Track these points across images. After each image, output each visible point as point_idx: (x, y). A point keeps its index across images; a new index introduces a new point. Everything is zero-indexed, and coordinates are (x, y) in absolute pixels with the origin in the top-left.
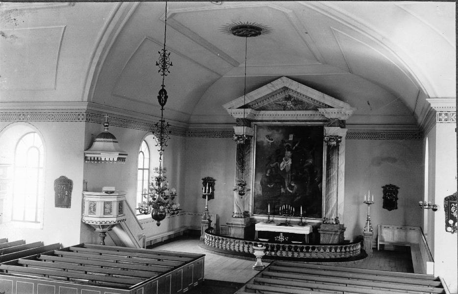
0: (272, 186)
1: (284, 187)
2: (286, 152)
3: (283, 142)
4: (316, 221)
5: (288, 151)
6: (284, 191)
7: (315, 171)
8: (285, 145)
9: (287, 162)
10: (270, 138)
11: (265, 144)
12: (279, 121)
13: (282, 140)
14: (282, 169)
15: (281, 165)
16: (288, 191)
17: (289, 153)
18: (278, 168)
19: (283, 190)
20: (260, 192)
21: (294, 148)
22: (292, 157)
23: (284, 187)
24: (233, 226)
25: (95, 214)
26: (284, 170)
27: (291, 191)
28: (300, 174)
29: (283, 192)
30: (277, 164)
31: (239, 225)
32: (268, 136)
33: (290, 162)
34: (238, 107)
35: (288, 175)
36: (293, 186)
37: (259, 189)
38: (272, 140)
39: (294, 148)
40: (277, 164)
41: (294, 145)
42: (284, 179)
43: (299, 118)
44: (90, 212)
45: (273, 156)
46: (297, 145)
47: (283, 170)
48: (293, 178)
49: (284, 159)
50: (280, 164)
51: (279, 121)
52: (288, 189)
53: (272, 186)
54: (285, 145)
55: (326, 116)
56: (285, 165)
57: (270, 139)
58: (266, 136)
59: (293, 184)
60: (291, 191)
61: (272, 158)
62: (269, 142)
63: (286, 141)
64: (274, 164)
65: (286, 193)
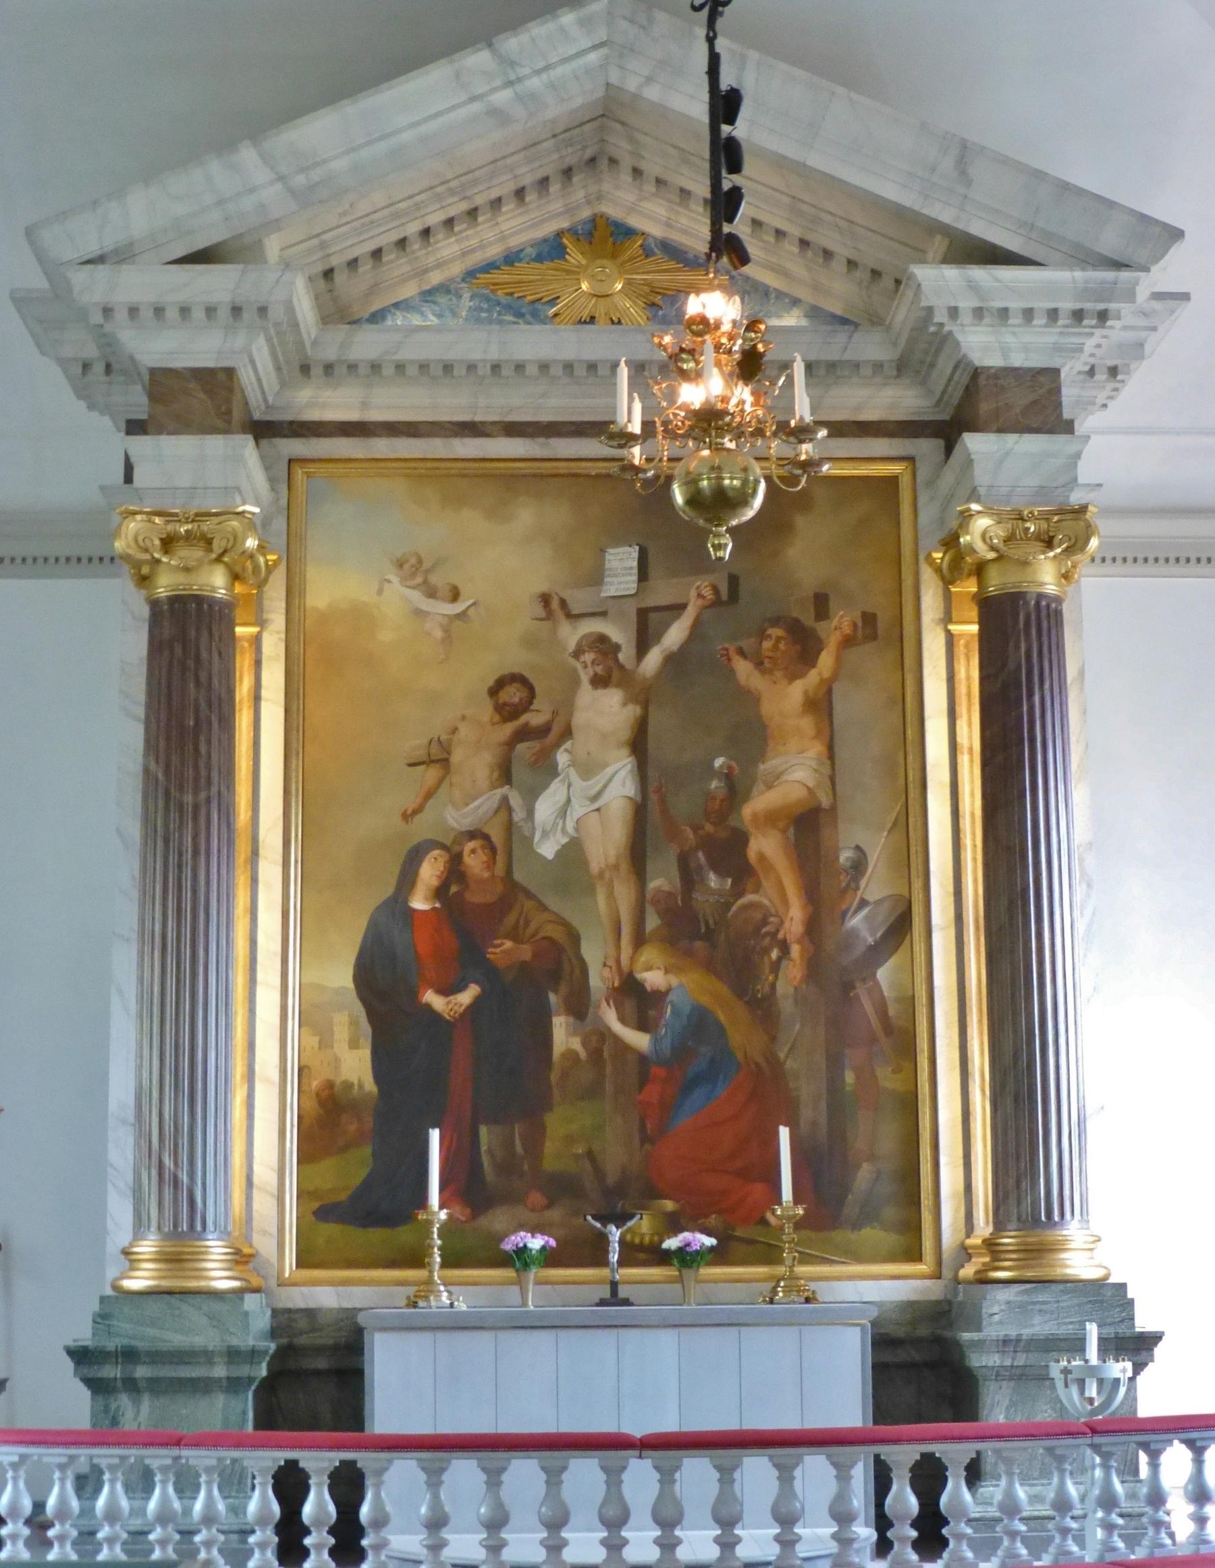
0: (466, 997)
1: (579, 1007)
2: (586, 695)
3: (551, 606)
4: (877, 1286)
5: (600, 682)
6: (576, 1044)
7: (845, 856)
8: (572, 635)
10: (435, 579)
11: (385, 636)
12: (513, 429)
13: (545, 599)
14: (548, 849)
15: (545, 808)
16: (617, 1039)
17: (604, 713)
18: (505, 839)
19: (564, 1036)
20: (356, 1066)
21: (654, 659)
22: (638, 744)
23: (579, 1007)
24: (141, 1372)
26: (573, 852)
27: (640, 1040)
28: (713, 880)
29: (571, 1055)
30: (505, 801)
31: (207, 1356)
32: (414, 568)
33: (620, 782)
34: (180, 253)
35: (611, 896)
36: (658, 997)
37: (341, 1033)
38: (455, 595)
39: (654, 659)
40: (505, 801)
41: (642, 647)
42: (575, 939)
45: (465, 731)
46: (675, 635)
47: (563, 853)
48: (652, 922)
49: (562, 758)
50: (530, 813)
51: (513, 429)
52: (611, 1017)
53: (466, 997)
54: (572, 635)
55: (983, 346)
56: (578, 809)
57: (431, 593)
58: (400, 564)
59: (654, 978)
60: (640, 1040)
61: (457, 757)
62: (419, 613)
63: (579, 600)
64: (487, 802)
65: (596, 1055)
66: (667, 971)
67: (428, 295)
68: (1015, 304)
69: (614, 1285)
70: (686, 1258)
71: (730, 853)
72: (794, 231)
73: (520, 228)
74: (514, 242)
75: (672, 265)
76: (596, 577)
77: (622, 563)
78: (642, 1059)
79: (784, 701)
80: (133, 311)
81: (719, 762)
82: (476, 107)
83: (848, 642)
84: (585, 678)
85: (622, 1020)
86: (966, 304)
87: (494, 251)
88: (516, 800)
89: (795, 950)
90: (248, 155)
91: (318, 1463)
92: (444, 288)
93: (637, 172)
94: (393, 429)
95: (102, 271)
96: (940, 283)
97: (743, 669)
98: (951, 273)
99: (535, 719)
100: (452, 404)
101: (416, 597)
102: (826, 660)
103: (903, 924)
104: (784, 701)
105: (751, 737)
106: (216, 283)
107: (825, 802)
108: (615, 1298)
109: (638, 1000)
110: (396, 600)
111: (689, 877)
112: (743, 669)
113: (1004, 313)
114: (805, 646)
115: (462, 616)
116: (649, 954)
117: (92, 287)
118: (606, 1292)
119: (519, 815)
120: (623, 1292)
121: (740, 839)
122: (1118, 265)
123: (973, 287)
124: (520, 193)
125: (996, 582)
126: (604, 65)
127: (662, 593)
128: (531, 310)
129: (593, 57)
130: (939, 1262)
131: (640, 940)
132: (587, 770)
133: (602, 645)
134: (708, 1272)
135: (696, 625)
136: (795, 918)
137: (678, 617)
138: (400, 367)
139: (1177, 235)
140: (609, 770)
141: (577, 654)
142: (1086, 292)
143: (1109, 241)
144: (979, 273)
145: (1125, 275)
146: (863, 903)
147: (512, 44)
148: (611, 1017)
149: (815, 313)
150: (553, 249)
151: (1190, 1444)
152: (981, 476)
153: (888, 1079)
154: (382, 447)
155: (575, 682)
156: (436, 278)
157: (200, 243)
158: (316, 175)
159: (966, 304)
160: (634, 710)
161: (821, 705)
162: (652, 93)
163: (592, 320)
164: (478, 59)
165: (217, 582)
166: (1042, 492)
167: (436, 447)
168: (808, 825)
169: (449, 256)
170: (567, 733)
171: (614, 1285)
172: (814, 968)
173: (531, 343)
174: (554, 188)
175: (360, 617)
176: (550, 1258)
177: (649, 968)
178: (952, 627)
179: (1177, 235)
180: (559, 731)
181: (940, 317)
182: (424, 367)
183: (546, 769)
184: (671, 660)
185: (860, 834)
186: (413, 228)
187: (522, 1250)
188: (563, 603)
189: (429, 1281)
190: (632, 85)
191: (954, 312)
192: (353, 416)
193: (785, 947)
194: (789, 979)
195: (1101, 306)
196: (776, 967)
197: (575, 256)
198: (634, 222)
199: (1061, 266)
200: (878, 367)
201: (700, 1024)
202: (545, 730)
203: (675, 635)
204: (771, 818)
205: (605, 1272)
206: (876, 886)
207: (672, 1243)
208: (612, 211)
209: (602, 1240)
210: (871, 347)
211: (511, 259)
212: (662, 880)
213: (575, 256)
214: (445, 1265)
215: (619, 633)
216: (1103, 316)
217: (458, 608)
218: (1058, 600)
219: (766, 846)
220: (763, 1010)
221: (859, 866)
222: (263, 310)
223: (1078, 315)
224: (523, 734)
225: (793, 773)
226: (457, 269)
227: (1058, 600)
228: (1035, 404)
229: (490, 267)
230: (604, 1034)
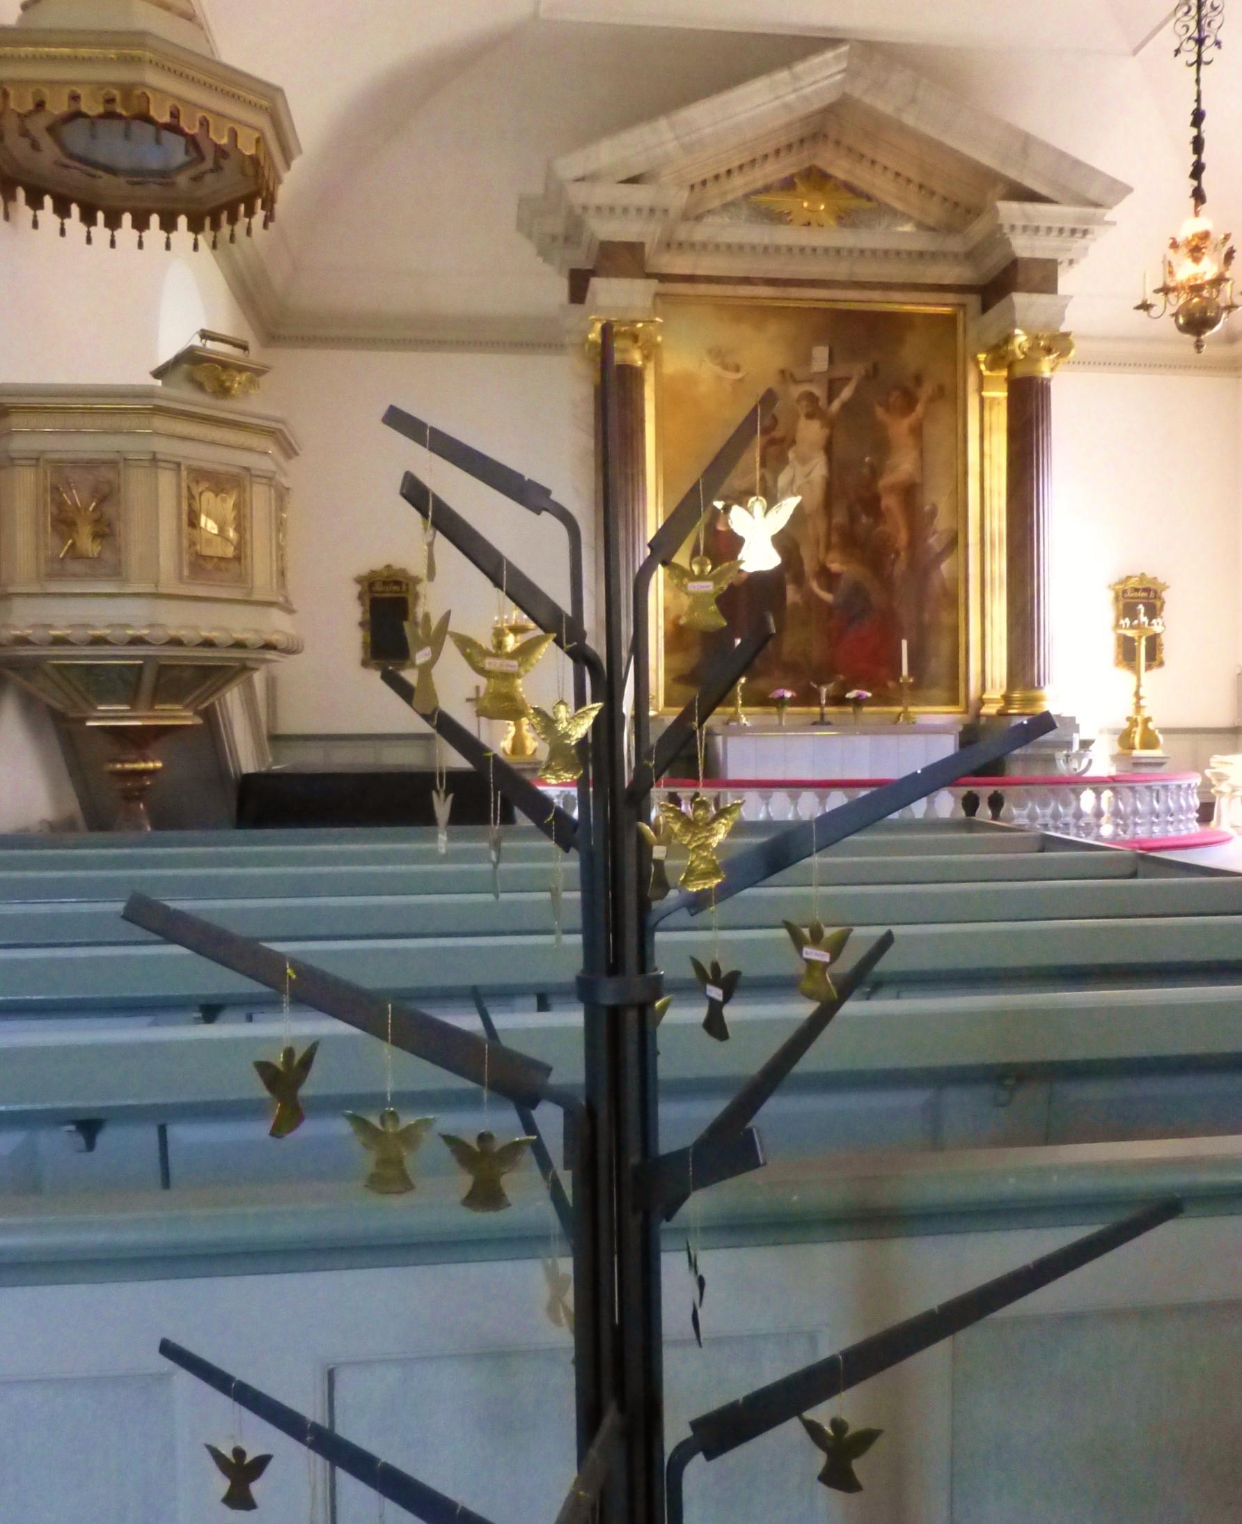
5: (810, 416)
7: (927, 508)
8: (796, 391)
9: (806, 469)
13: (782, 372)
17: (811, 432)
21: (836, 405)
22: (829, 448)
25: (117, 572)
27: (827, 597)
28: (864, 519)
29: (795, 604)
32: (718, 355)
34: (625, 178)
36: (837, 576)
38: (737, 369)
39: (836, 405)
41: (830, 400)
43: (866, 271)
44: (65, 564)
46: (846, 393)
49: (791, 455)
50: (776, 481)
52: (815, 586)
54: (796, 391)
55: (1023, 247)
57: (725, 367)
59: (835, 567)
60: (827, 597)
63: (799, 373)
66: (842, 564)
67: (726, 207)
68: (1043, 225)
69: (822, 715)
70: (858, 702)
71: (872, 504)
72: (917, 179)
73: (773, 171)
74: (770, 180)
75: (849, 195)
76: (808, 359)
77: (821, 355)
78: (830, 608)
79: (899, 428)
80: (599, 209)
81: (867, 459)
82: (777, 103)
83: (932, 400)
84: (802, 412)
85: (821, 587)
86: (1019, 223)
87: (759, 184)
88: (769, 476)
89: (903, 554)
90: (663, 123)
91: (985, 792)
92: (733, 204)
93: (838, 143)
94: (709, 280)
95: (583, 185)
96: (1010, 210)
97: (880, 412)
98: (1015, 206)
99: (778, 433)
100: (738, 267)
101: (718, 370)
102: (920, 408)
103: (956, 541)
104: (899, 428)
105: (882, 447)
106: (640, 195)
107: (918, 480)
108: (822, 722)
109: (828, 578)
110: (707, 371)
111: (853, 518)
112: (880, 412)
113: (1037, 229)
114: (909, 401)
115: (741, 380)
116: (833, 555)
117: (579, 195)
118: (818, 718)
119: (770, 483)
120: (827, 718)
121: (876, 499)
122: (1097, 205)
123: (1025, 215)
124: (777, 152)
125: (1020, 371)
126: (843, 82)
127: (840, 372)
128: (777, 218)
129: (839, 77)
130: (967, 706)
131: (828, 548)
132: (804, 460)
133: (811, 397)
134: (789, 709)
135: (857, 389)
136: (903, 537)
137: (846, 385)
138: (717, 247)
139: (1128, 190)
140: (814, 462)
141: (798, 401)
142: (1080, 219)
143: (1093, 193)
144: (1029, 207)
145: (1099, 211)
146: (934, 533)
147: (800, 68)
148: (815, 586)
149: (921, 226)
150: (788, 185)
151: (1113, 789)
152: (1018, 316)
153: (945, 618)
154: (702, 289)
155: (798, 416)
156: (730, 198)
157: (635, 172)
158: (694, 137)
159: (1019, 223)
160: (826, 431)
161: (917, 432)
162: (868, 100)
163: (809, 224)
164: (783, 75)
165: (637, 358)
166: (1047, 326)
167: (729, 290)
168: (910, 492)
169: (739, 185)
170: (794, 442)
171: (822, 715)
172: (913, 563)
173: (784, 235)
174: (794, 150)
175: (689, 379)
176: (794, 702)
177: (833, 562)
178: (985, 394)
179: (1128, 190)
180: (788, 441)
181: (1006, 230)
182: (729, 246)
183: (782, 461)
184: (845, 406)
185: (936, 497)
186: (723, 170)
187: (783, 697)
188: (792, 375)
189: (736, 713)
190: (857, 93)
191: (1013, 227)
192: (687, 271)
193: (898, 554)
194: (900, 567)
195: (1085, 227)
196: (894, 562)
197: (801, 188)
198: (832, 171)
199: (1069, 204)
200: (956, 255)
201: (857, 589)
202: (782, 441)
203: (846, 393)
204: (892, 488)
205: (817, 709)
206: (942, 522)
207: (851, 695)
208: (820, 163)
209: (818, 694)
210: (954, 244)
211: (767, 189)
212: (840, 518)
213: (801, 188)
214: (744, 705)
215: (819, 391)
216: (1085, 232)
217: (739, 376)
218: (1049, 380)
219: (890, 502)
220: (887, 584)
221: (933, 513)
222: (666, 211)
223: (1073, 231)
224: (772, 442)
225: (903, 465)
226: (740, 193)
227: (1049, 380)
228: (1043, 277)
229: (757, 192)
230: (810, 597)
